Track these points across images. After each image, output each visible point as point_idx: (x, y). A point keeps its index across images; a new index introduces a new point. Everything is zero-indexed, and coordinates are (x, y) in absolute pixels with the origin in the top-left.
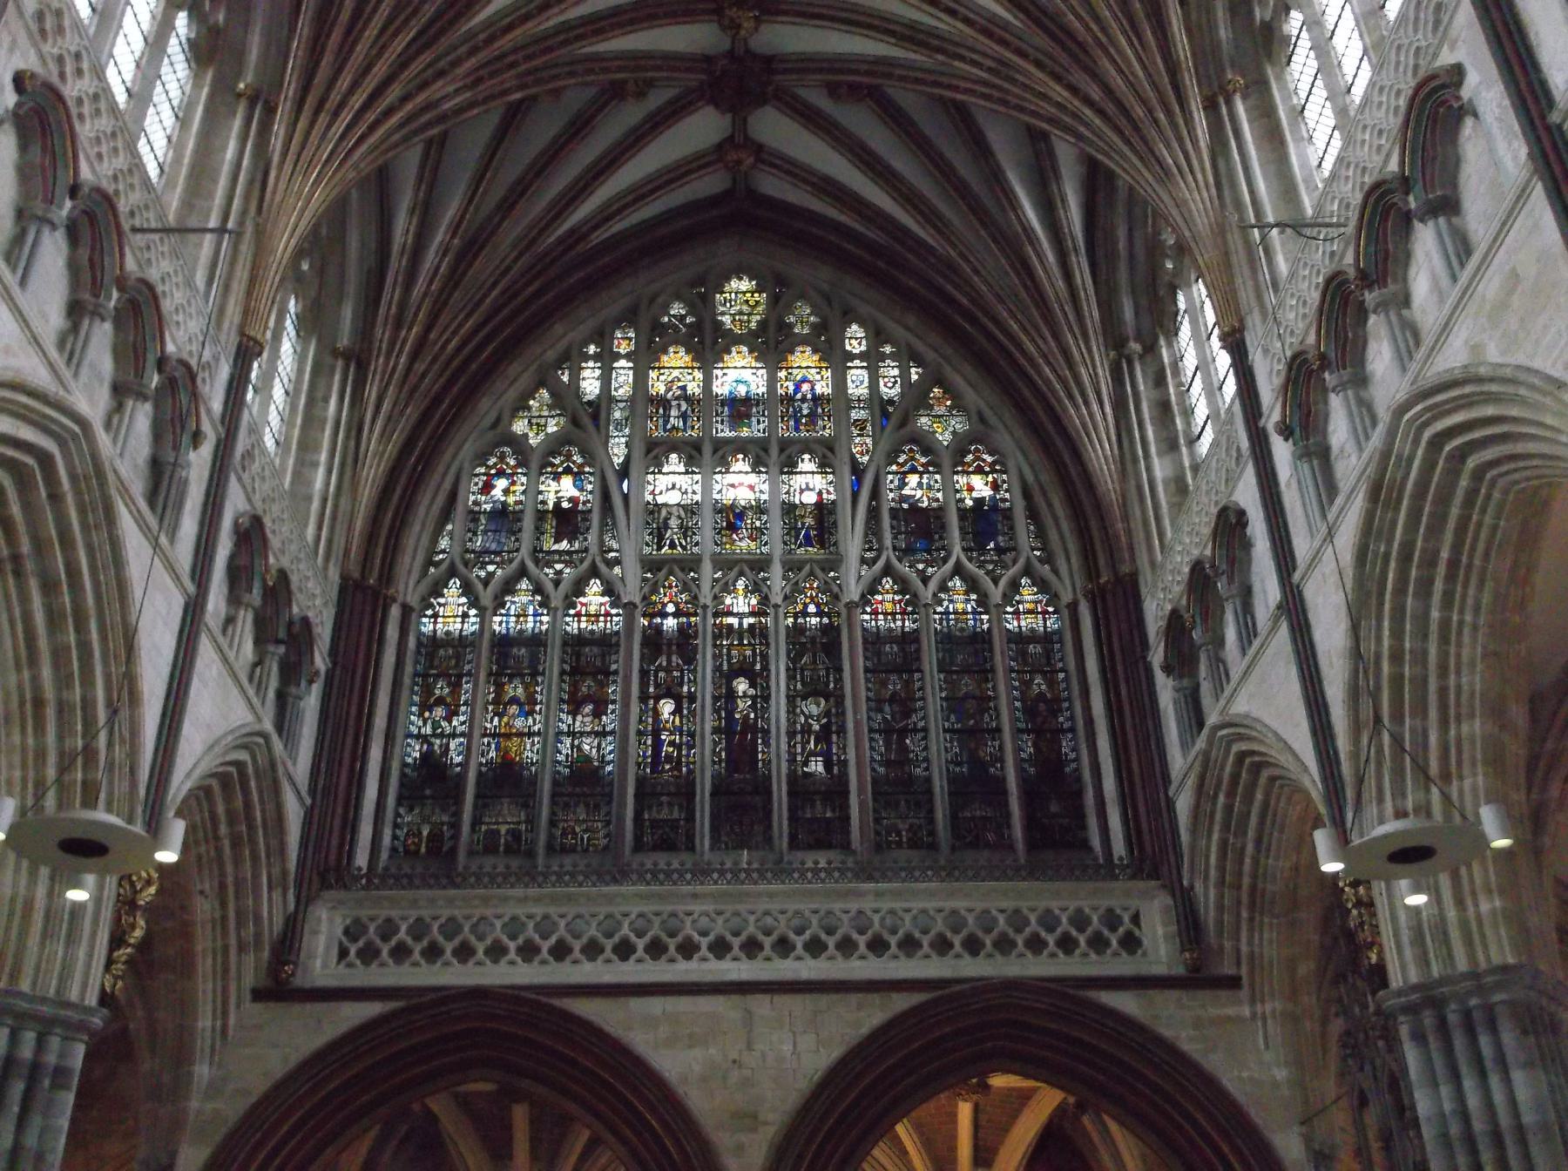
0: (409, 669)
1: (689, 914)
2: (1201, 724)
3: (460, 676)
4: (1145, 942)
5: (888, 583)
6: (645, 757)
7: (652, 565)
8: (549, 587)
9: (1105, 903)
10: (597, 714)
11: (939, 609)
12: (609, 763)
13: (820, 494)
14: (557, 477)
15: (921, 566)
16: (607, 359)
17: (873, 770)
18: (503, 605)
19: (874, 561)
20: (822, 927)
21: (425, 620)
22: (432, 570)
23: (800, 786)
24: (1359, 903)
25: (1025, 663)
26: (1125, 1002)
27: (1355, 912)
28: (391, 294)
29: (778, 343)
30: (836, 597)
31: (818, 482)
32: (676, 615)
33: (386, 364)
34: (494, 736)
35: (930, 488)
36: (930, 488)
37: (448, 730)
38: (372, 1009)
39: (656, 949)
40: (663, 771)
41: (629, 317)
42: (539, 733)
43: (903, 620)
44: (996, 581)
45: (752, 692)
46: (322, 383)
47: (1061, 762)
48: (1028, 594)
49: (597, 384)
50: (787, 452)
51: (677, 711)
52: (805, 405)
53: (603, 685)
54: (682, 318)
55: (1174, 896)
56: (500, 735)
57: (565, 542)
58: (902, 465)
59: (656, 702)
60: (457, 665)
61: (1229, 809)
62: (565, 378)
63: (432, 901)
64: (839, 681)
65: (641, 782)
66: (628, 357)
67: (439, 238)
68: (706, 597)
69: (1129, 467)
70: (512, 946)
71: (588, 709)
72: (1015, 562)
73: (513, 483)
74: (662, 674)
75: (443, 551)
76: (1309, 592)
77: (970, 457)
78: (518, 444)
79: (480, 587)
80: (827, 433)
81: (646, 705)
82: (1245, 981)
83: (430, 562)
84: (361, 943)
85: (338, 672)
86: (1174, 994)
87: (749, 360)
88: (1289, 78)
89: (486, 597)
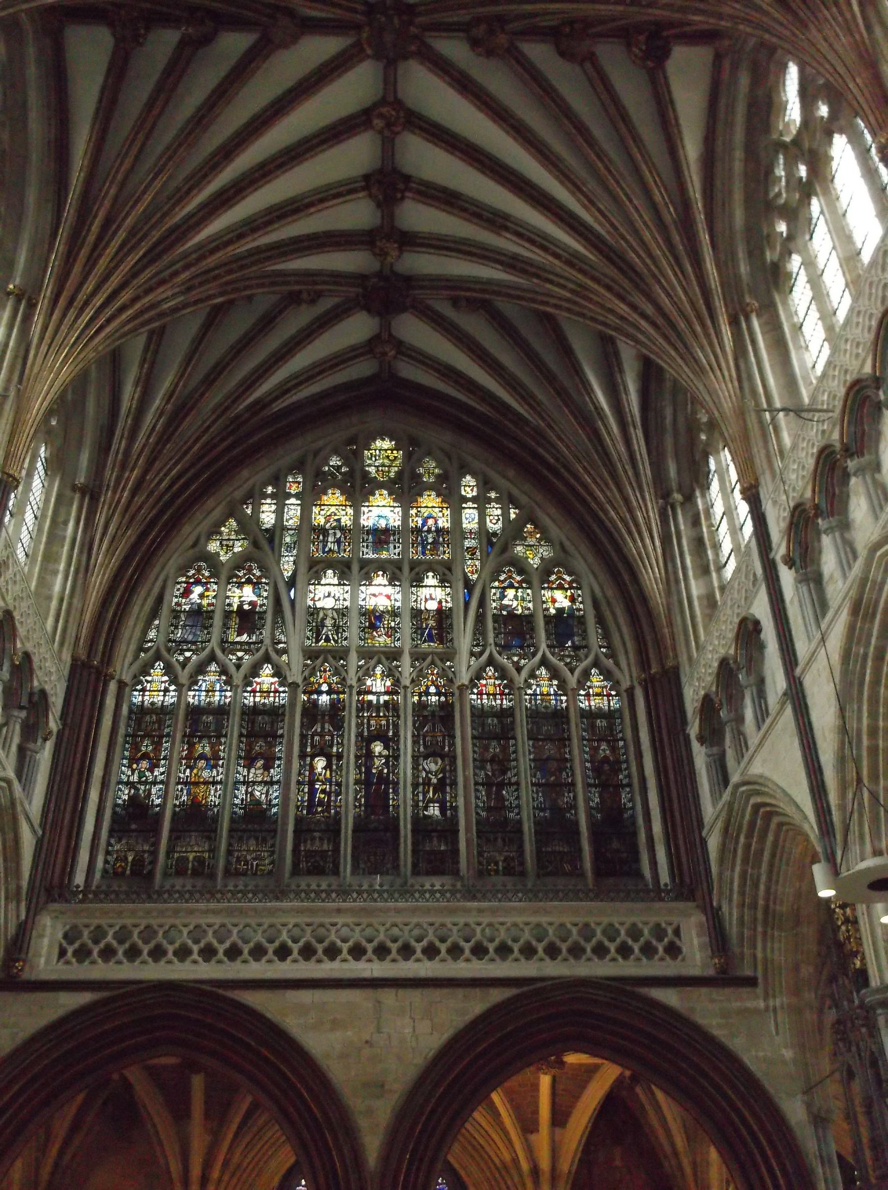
0: (122, 731)
1: (334, 925)
2: (726, 781)
3: (161, 737)
4: (684, 950)
5: (490, 671)
6: (302, 801)
7: (311, 654)
8: (232, 669)
9: (654, 920)
10: (267, 767)
11: (529, 692)
12: (274, 806)
13: (440, 602)
14: (240, 585)
15: (516, 659)
16: (281, 497)
17: (477, 813)
18: (196, 683)
19: (481, 654)
20: (436, 936)
21: (135, 693)
22: (143, 655)
23: (422, 826)
24: (847, 921)
25: (594, 734)
26: (670, 997)
27: (843, 928)
28: (119, 444)
29: (410, 488)
30: (451, 681)
31: (439, 593)
32: (329, 693)
33: (113, 498)
34: (186, 783)
35: (523, 599)
36: (523, 599)
37: (151, 779)
38: (85, 998)
39: (308, 952)
40: (317, 812)
41: (299, 467)
42: (221, 782)
43: (502, 700)
44: (572, 671)
45: (385, 752)
46: (63, 510)
47: (621, 810)
48: (596, 681)
49: (273, 516)
50: (417, 570)
51: (328, 766)
52: (430, 536)
53: (272, 746)
54: (338, 468)
55: (706, 914)
56: (191, 783)
57: (245, 635)
58: (503, 582)
59: (312, 759)
60: (159, 728)
61: (748, 846)
62: (249, 511)
63: (133, 913)
64: (452, 745)
65: (299, 821)
66: (297, 496)
67: (157, 402)
68: (352, 680)
69: (673, 584)
70: (195, 948)
71: (260, 763)
72: (586, 657)
73: (207, 590)
74: (317, 738)
75: (151, 641)
76: (807, 682)
77: (553, 577)
78: (211, 560)
79: (178, 668)
80: (446, 557)
81: (305, 761)
82: (760, 980)
83: (141, 649)
84: (77, 945)
85: (67, 732)
86: (704, 990)
87: (389, 501)
88: (790, 302)
89: (184, 676)
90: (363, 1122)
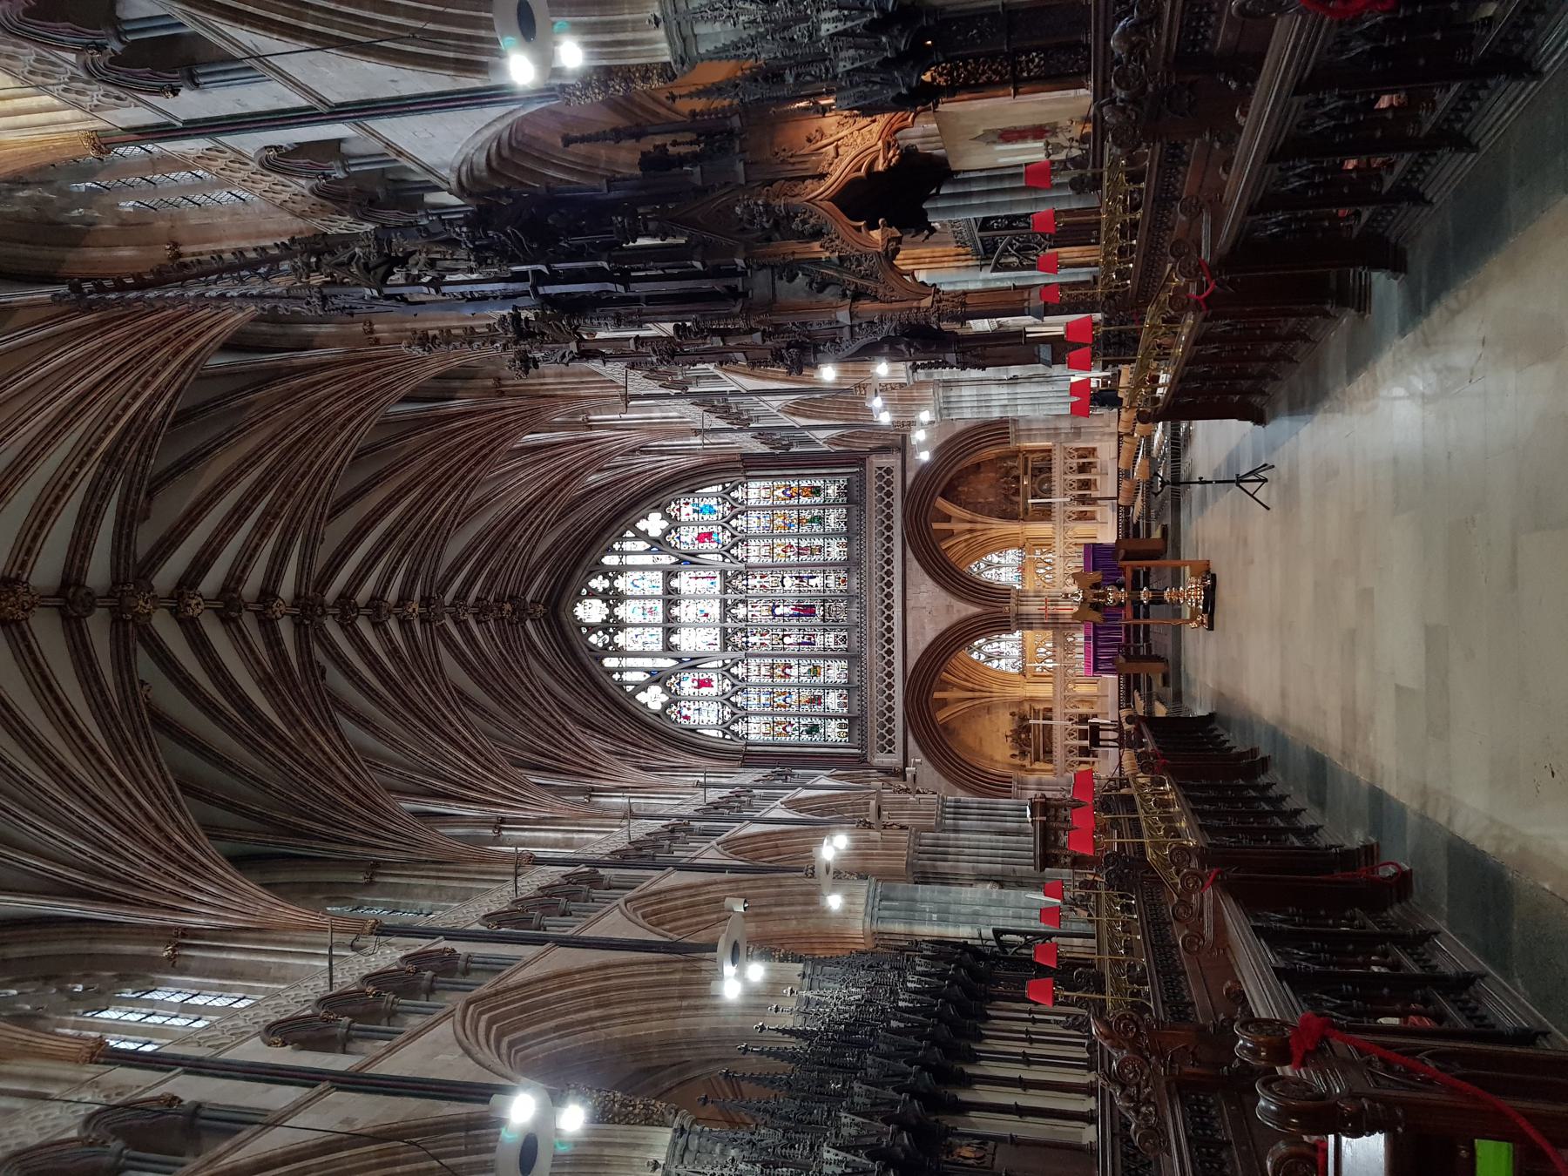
8: (736, 688)
10: (790, 667)
16: (621, 671)
41: (599, 660)
68: (740, 625)
71: (787, 671)
78: (666, 706)
80: (660, 574)
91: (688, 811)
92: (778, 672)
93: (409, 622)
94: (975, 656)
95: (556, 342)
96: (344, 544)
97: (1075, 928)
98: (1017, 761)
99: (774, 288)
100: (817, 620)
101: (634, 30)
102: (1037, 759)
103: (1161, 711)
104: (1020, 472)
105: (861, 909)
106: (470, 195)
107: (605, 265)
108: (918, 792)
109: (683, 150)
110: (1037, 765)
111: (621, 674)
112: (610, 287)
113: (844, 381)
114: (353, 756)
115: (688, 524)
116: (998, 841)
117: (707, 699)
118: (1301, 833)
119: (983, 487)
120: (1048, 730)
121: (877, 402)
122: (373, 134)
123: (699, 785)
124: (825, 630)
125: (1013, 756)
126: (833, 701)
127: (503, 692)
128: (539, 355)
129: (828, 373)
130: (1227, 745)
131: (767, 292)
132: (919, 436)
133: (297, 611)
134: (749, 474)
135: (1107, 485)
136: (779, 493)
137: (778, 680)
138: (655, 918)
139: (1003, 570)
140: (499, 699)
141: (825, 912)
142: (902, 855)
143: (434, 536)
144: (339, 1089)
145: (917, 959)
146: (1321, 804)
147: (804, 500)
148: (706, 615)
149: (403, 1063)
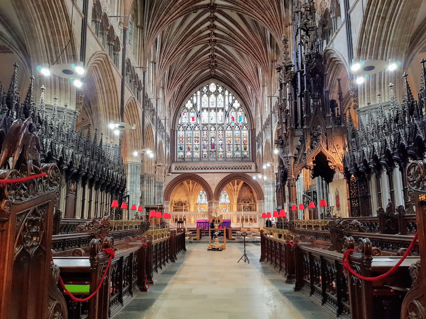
8: (192, 128)
10: (198, 142)
16: (196, 96)
22: (179, 125)
38: (179, 174)
39: (205, 169)
41: (199, 90)
68: (209, 129)
71: (197, 141)
78: (187, 108)
80: (223, 107)
90: (212, 188)
91: (159, 115)
92: (196, 139)
93: (209, 36)
94: (201, 192)
95: (285, 77)
96: (231, 18)
97: (130, 216)
98: (173, 202)
99: (298, 136)
100: (210, 149)
101: (367, 98)
102: (174, 208)
103: (187, 238)
104: (250, 203)
105: (134, 161)
106: (325, 53)
107: (305, 90)
108: (165, 176)
109: (336, 111)
110: (172, 208)
111: (196, 96)
112: (299, 92)
113: (274, 156)
114: (173, 21)
115: (237, 114)
116: (152, 197)
117: (189, 120)
118: (156, 268)
119: (246, 194)
120: (181, 210)
121: (269, 165)
122: (342, 26)
123: (166, 117)
124: (208, 152)
125: (175, 201)
126: (189, 154)
127: (190, 63)
128: (281, 72)
129: (276, 151)
130: (178, 253)
131: (297, 134)
132: (260, 176)
133: (212, 5)
134: (250, 131)
135: (246, 225)
136: (245, 139)
137: (194, 139)
138: (130, 105)
139: (224, 199)
140: (188, 62)
141: (132, 150)
142: (148, 172)
143: (233, 43)
144: (83, 20)
145: (121, 175)
146: (163, 273)
147: (243, 146)
148: (212, 119)
149: (90, 37)
